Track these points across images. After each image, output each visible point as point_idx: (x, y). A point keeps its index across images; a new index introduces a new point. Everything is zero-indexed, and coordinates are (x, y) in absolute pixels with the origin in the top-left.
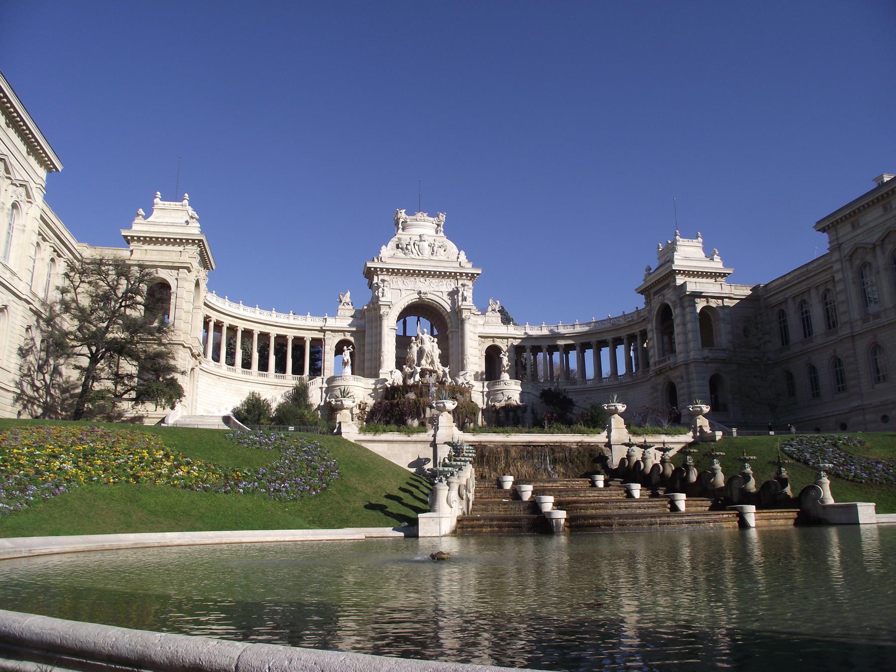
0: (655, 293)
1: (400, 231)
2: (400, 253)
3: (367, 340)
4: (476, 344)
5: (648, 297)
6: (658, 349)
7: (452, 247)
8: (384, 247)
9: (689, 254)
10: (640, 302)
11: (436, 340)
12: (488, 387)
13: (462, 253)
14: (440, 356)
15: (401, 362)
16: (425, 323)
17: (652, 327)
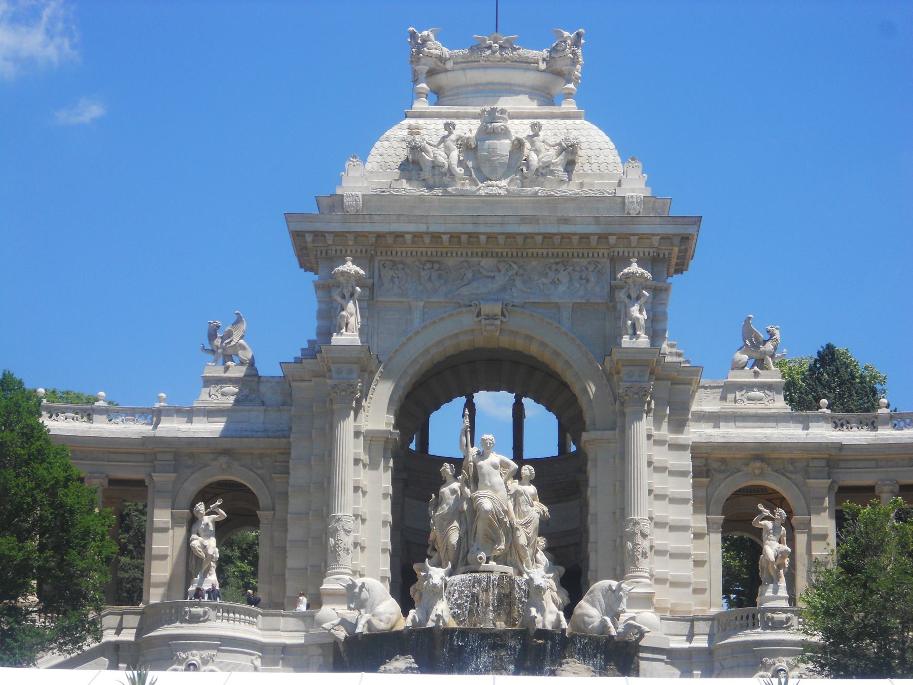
1: (421, 105)
14: (544, 528)
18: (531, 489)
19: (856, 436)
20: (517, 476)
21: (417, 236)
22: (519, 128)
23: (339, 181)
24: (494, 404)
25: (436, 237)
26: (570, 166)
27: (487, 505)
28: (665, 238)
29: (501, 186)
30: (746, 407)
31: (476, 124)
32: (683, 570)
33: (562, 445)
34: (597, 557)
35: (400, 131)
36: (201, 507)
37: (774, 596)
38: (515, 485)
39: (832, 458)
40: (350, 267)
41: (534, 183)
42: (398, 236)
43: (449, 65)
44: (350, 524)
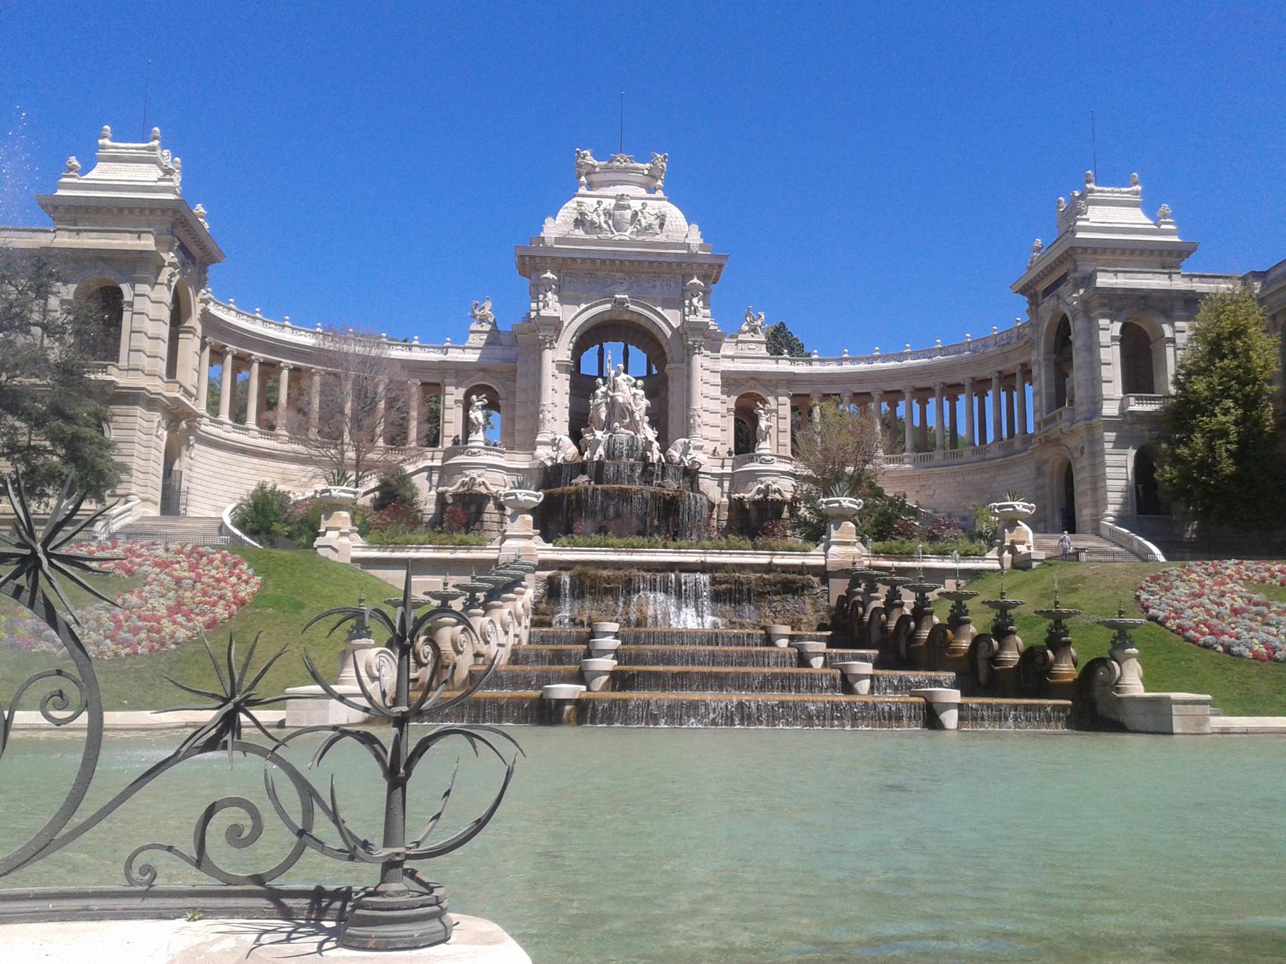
0: (1047, 292)
1: (582, 190)
2: (580, 233)
3: (521, 383)
4: (717, 391)
5: (1034, 302)
6: (1048, 396)
7: (675, 215)
8: (549, 220)
9: (1113, 215)
10: (1017, 314)
11: (640, 383)
12: (733, 468)
13: (695, 227)
15: (579, 424)
16: (639, 357)
17: (1038, 358)
18: (642, 392)
19: (801, 368)
20: (635, 385)
21: (583, 260)
22: (636, 205)
23: (542, 229)
24: (613, 350)
25: (593, 261)
26: (662, 225)
27: (621, 400)
28: (711, 265)
29: (627, 235)
30: (747, 353)
31: (613, 202)
32: (716, 433)
33: (649, 370)
34: (672, 428)
35: (572, 204)
36: (474, 397)
37: (765, 447)
38: (634, 390)
39: (790, 380)
40: (549, 275)
41: (643, 234)
42: (574, 259)
43: (597, 170)
44: (551, 408)
